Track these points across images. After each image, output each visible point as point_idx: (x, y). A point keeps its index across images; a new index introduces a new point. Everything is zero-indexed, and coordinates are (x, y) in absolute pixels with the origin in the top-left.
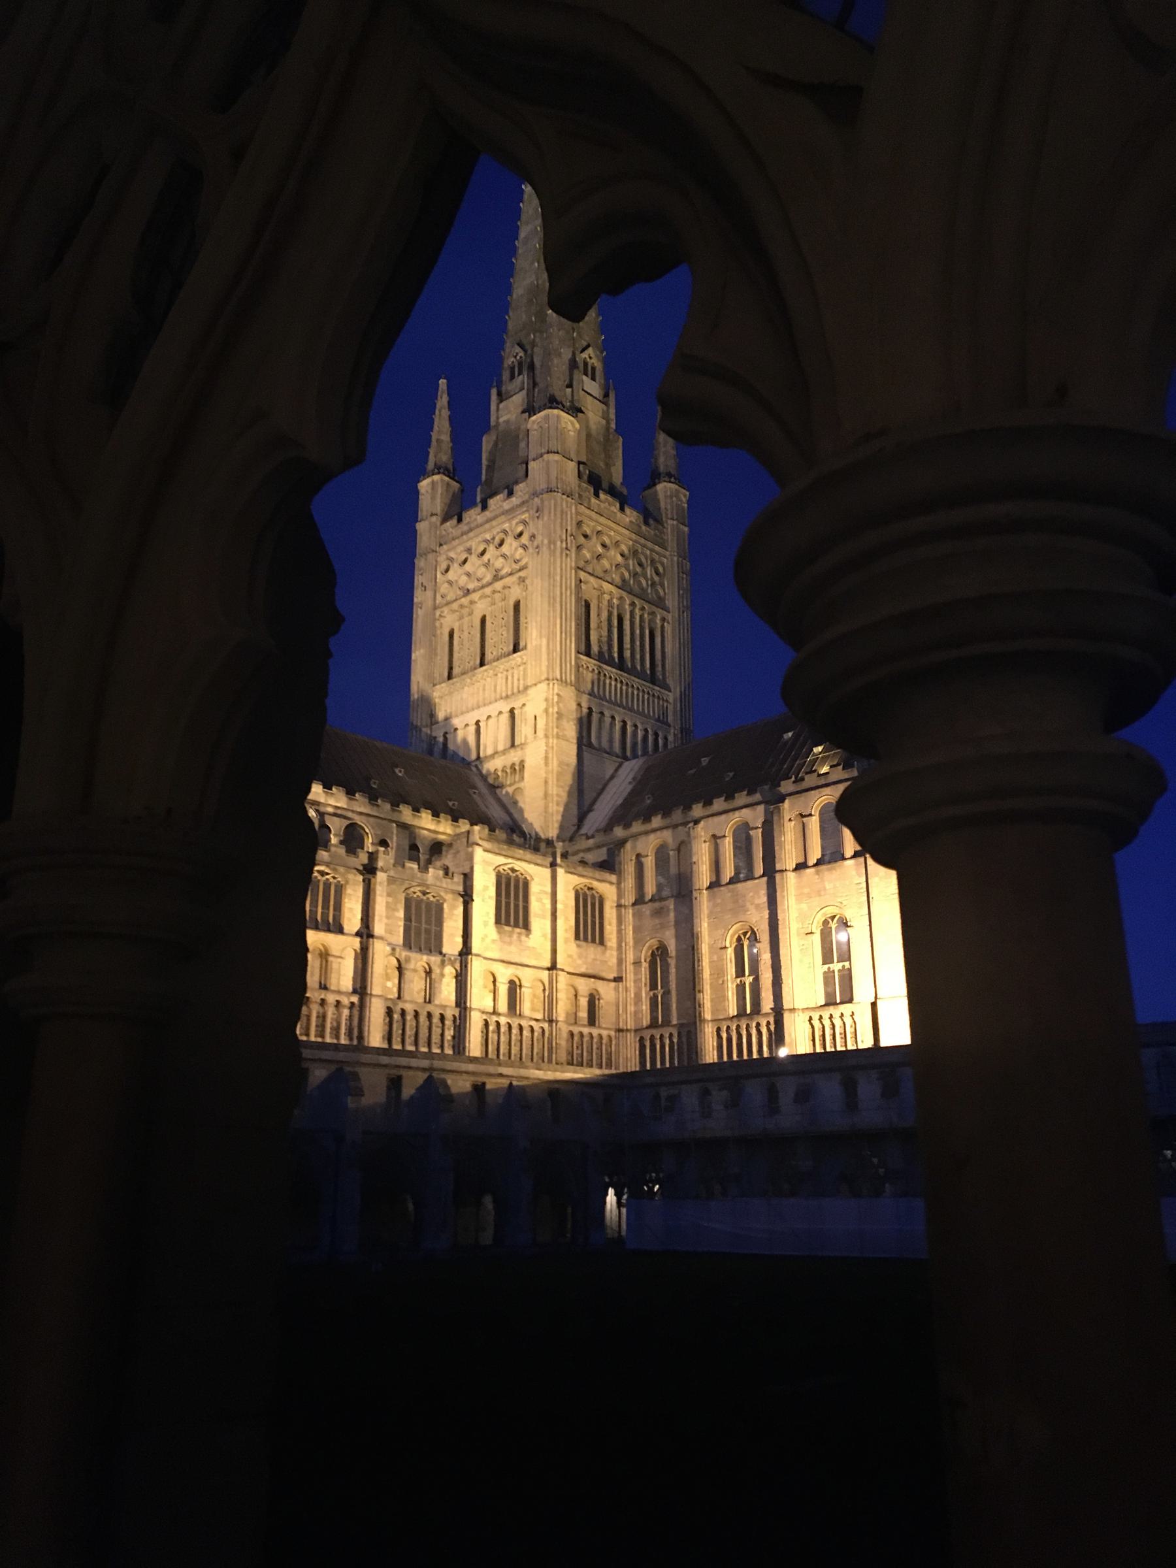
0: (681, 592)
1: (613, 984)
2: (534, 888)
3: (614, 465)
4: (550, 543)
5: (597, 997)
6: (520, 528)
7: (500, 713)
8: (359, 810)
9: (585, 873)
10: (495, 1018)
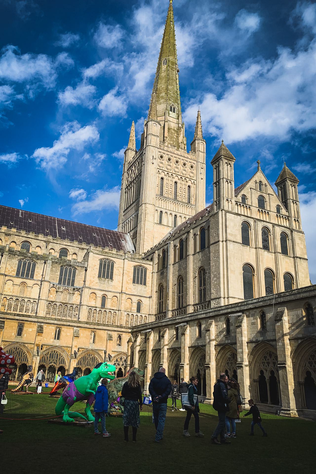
1: (148, 299)
2: (115, 266)
5: (141, 303)
8: (65, 244)
9: (138, 261)
10: (94, 308)
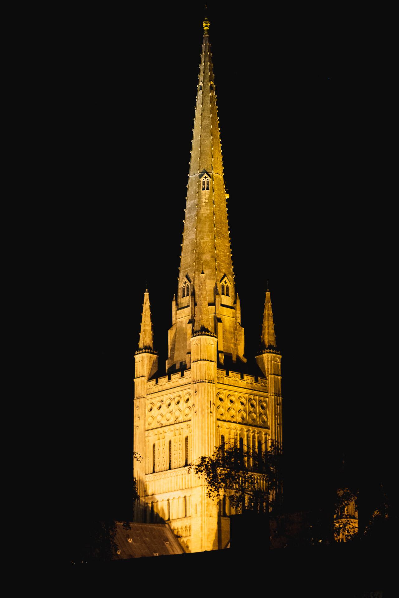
0: (276, 416)
3: (240, 345)
4: (202, 410)
6: (187, 397)
7: (179, 497)
